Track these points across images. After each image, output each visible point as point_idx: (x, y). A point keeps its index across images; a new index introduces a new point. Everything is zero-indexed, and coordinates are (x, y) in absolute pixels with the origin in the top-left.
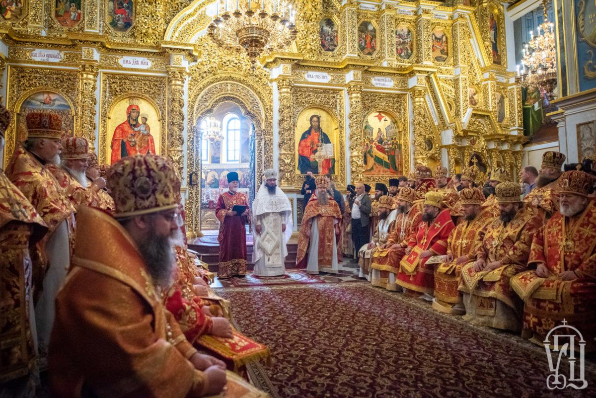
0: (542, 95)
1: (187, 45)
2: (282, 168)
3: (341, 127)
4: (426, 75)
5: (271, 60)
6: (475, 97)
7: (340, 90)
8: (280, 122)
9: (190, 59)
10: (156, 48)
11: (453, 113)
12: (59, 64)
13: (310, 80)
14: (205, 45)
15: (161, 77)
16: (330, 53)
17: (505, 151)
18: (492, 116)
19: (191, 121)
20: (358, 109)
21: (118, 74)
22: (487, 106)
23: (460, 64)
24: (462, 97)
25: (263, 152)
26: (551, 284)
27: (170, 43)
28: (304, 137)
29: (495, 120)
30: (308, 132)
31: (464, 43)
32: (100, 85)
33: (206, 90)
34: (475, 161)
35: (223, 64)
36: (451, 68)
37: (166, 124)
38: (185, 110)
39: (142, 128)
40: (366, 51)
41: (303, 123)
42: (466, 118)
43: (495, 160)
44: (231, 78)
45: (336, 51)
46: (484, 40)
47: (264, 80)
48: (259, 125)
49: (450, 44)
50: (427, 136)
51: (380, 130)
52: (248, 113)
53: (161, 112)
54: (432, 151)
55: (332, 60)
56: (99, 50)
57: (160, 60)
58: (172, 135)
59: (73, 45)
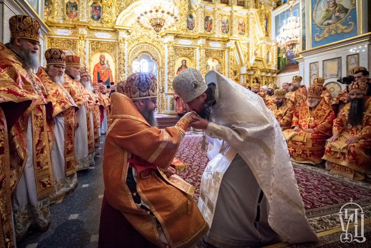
0: (287, 51)
1: (126, 27)
2: (169, 84)
3: (196, 65)
4: (235, 41)
5: (165, 34)
6: (257, 52)
7: (195, 48)
8: (168, 63)
9: (128, 33)
10: (112, 28)
11: (246, 59)
12: (69, 36)
13: (182, 43)
14: (134, 27)
15: (114, 42)
16: (191, 31)
17: (269, 77)
18: (264, 60)
19: (128, 62)
20: (204, 57)
21: (95, 41)
22: (261, 56)
23: (250, 36)
24: (251, 52)
25: (160, 77)
26: (301, 134)
27: (119, 26)
28: (179, 70)
29: (265, 62)
30: (181, 68)
31: (252, 26)
32: (87, 46)
33: (135, 48)
34: (255, 81)
35: (142, 37)
36: (246, 38)
37: (117, 64)
38: (126, 57)
39: (106, 66)
40: (208, 30)
41: (178, 64)
42: (252, 61)
43: (264, 81)
44: (146, 43)
45: (194, 30)
46: (262, 24)
47: (161, 44)
48: (158, 64)
49: (246, 27)
50: (234, 70)
51: (213, 67)
52: (154, 59)
53: (115, 58)
54: (236, 76)
55: (192, 34)
56: (86, 29)
57: (114, 34)
58: (120, 69)
59: (75, 27)
